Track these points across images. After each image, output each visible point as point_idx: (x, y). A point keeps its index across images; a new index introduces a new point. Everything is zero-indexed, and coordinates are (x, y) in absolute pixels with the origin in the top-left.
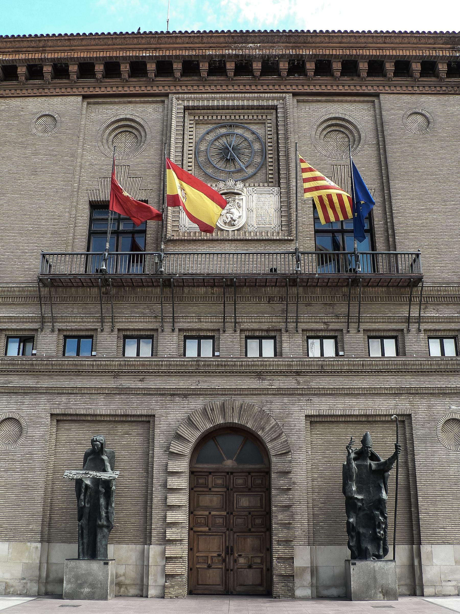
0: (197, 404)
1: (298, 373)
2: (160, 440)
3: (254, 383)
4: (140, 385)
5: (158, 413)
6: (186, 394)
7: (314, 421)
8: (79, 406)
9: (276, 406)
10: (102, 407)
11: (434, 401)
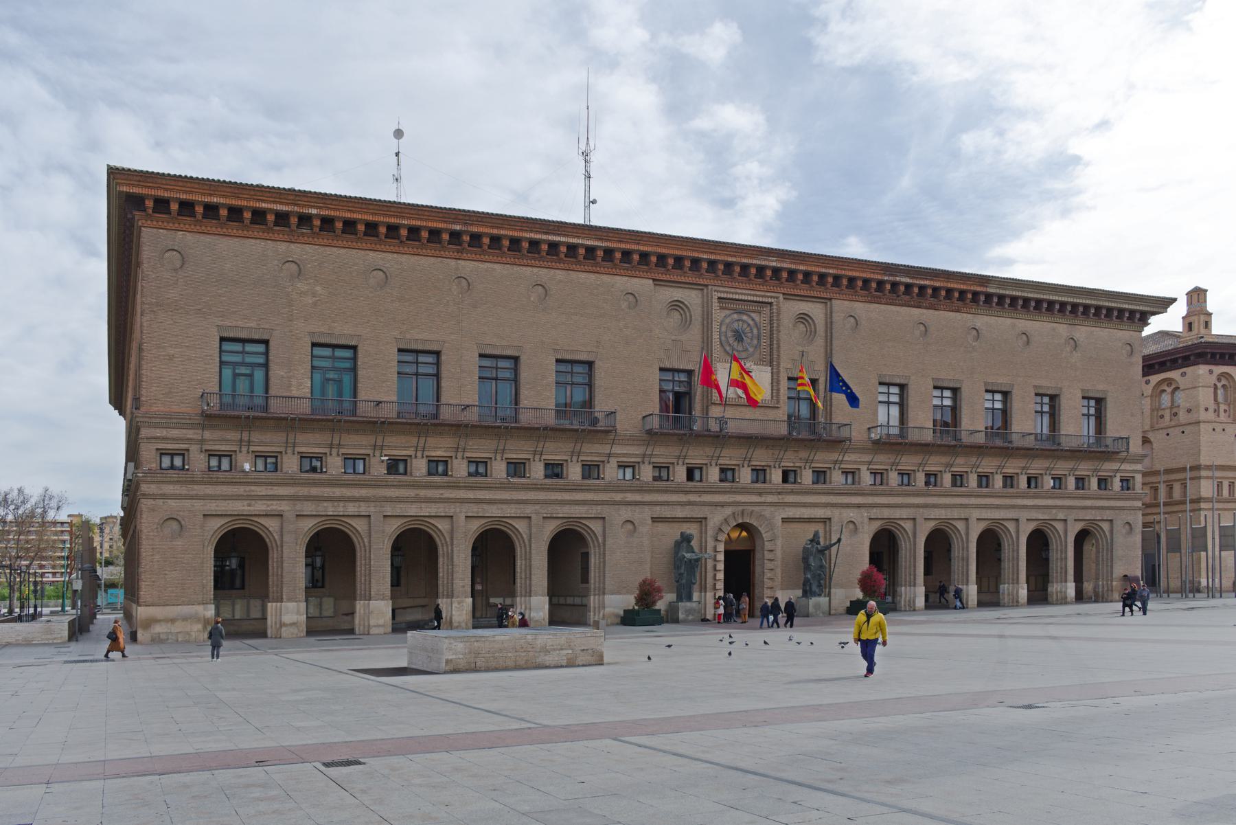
0: (728, 511)
1: (779, 493)
2: (710, 533)
3: (755, 499)
4: (698, 499)
5: (709, 516)
6: (723, 505)
7: (785, 520)
8: (667, 512)
9: (767, 511)
10: (680, 513)
11: (843, 510)
